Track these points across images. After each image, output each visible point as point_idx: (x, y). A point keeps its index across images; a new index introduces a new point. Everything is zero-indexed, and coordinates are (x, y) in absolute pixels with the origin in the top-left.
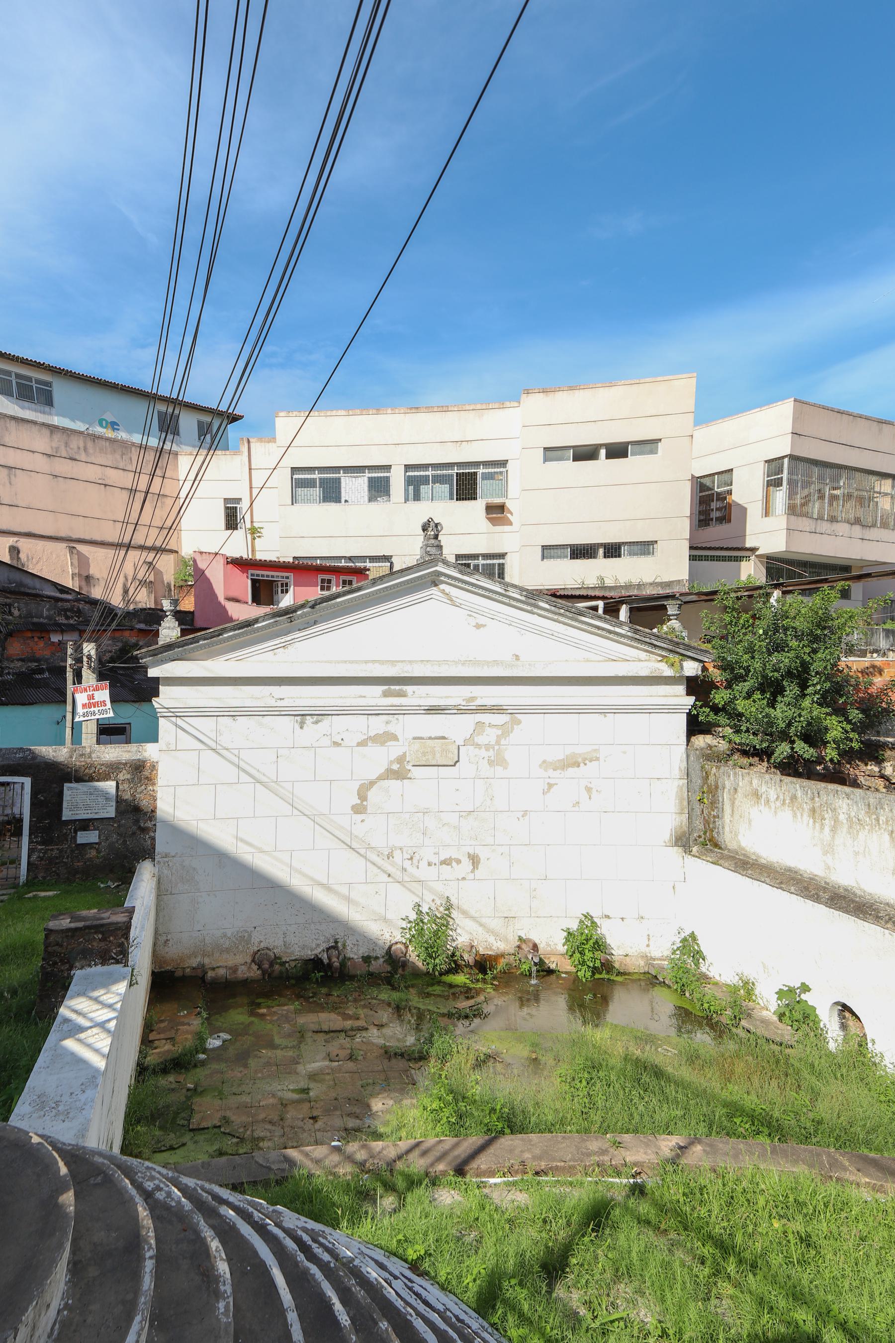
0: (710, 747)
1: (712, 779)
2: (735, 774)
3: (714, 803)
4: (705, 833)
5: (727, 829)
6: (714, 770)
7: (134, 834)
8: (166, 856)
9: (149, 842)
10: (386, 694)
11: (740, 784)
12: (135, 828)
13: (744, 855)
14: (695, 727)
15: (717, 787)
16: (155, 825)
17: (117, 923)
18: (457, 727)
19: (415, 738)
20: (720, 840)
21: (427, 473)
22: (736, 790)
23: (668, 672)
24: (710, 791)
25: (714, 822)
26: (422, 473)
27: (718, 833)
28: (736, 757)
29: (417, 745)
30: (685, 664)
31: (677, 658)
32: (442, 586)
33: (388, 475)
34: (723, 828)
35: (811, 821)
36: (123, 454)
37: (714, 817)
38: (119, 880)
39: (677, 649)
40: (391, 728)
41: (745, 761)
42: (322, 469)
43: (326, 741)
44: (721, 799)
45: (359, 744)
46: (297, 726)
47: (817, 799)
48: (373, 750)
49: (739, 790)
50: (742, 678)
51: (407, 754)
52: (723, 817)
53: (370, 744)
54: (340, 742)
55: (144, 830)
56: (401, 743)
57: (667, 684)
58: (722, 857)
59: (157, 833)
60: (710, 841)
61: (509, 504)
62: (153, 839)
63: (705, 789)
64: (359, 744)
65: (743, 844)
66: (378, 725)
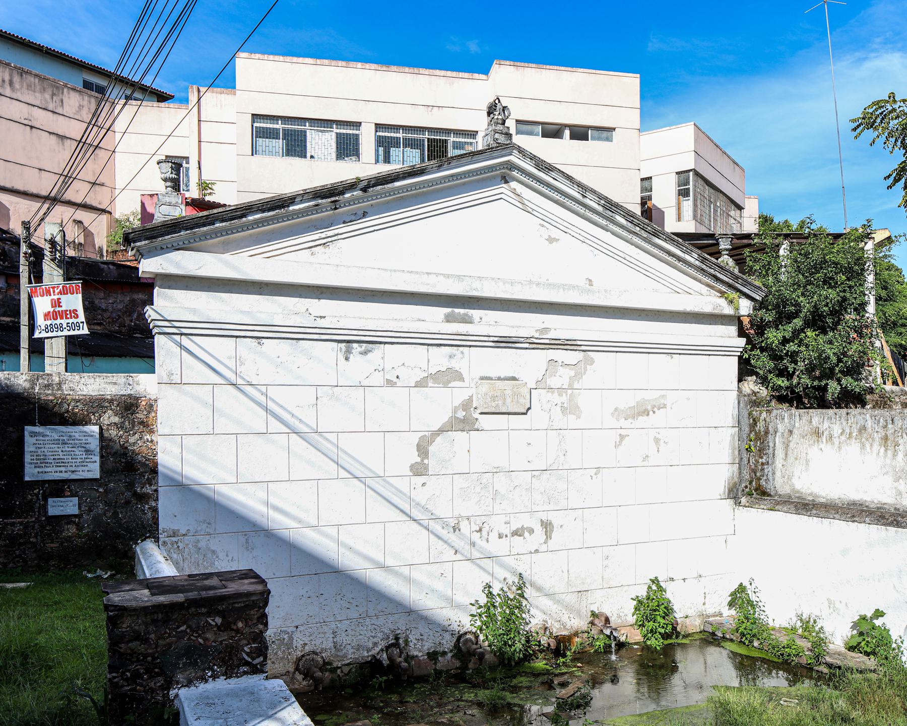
0: (754, 392)
1: (760, 426)
3: (761, 451)
4: (751, 483)
5: (778, 474)
6: (764, 415)
7: (128, 502)
8: (174, 534)
9: (150, 515)
11: (797, 425)
12: (128, 494)
14: (745, 369)
15: (767, 432)
16: (156, 491)
18: (528, 365)
19: (482, 378)
20: (769, 487)
22: (791, 432)
23: (728, 310)
24: (758, 437)
25: (763, 470)
27: (767, 480)
28: (773, 403)
29: (485, 387)
30: (740, 300)
31: (733, 295)
34: (774, 474)
38: (111, 568)
39: (732, 287)
40: (455, 364)
43: (378, 379)
44: (771, 445)
45: (420, 384)
48: (434, 392)
49: (795, 431)
51: (474, 399)
52: (773, 463)
53: (430, 384)
54: (395, 380)
55: (143, 498)
56: (466, 384)
59: (160, 502)
60: (756, 490)
62: (155, 510)
63: (752, 436)
64: (420, 384)
66: (439, 358)
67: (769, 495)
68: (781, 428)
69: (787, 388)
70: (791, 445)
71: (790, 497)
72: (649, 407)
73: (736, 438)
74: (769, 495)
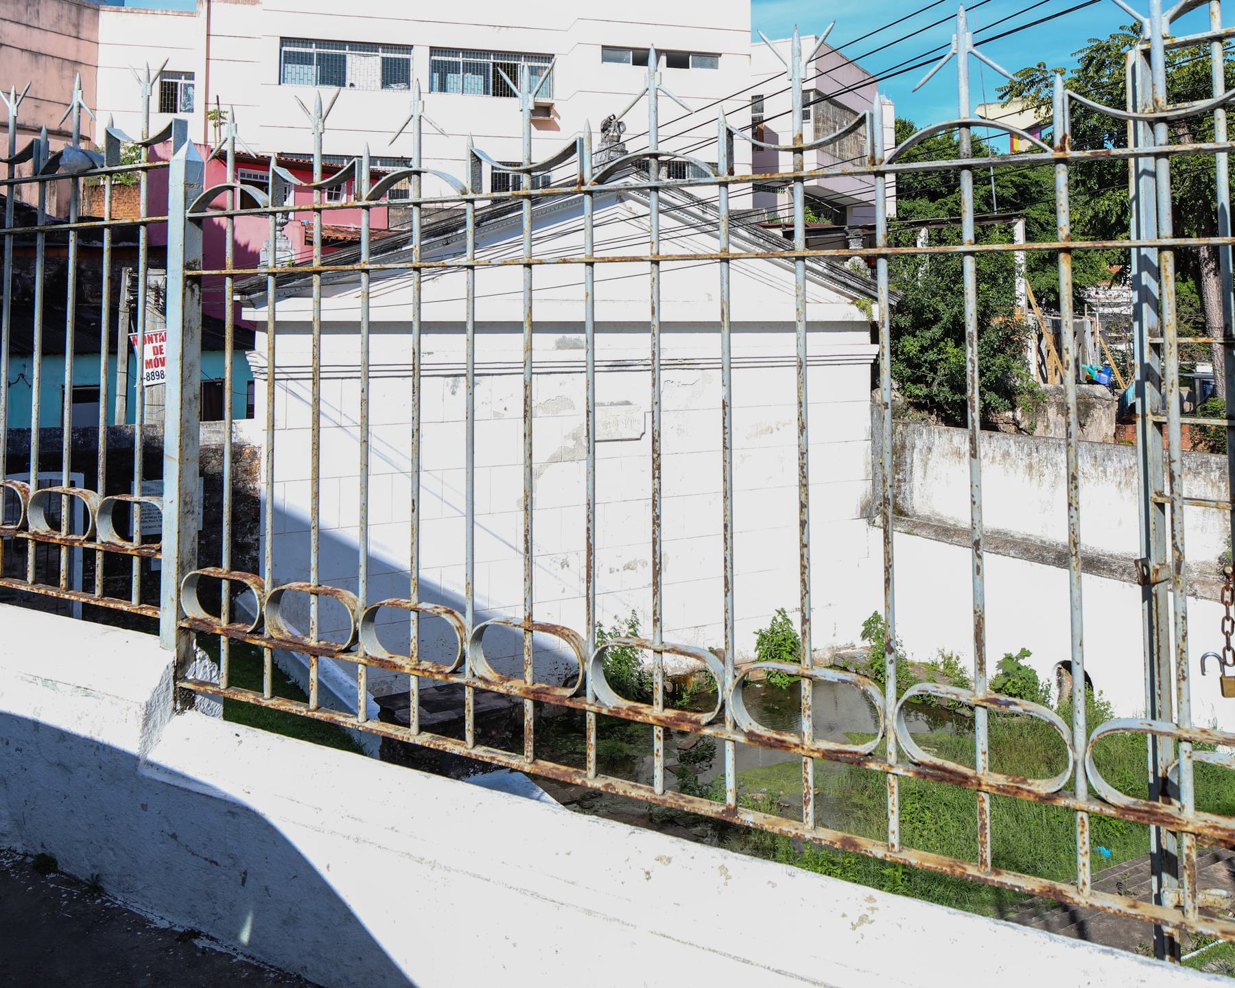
2: (930, 431)
10: (561, 346)
13: (939, 521)
15: (903, 447)
17: (501, 710)
20: (906, 506)
21: (457, 59)
22: (930, 449)
25: (899, 487)
26: (450, 59)
28: (910, 412)
32: (629, 203)
33: (407, 56)
34: (911, 492)
35: (1027, 477)
36: (28, 5)
37: (899, 480)
41: (919, 415)
42: (321, 43)
44: (908, 460)
46: (448, 391)
47: (1035, 454)
50: (928, 325)
52: (911, 480)
57: (853, 330)
58: (916, 526)
61: (556, 108)
65: (937, 510)
67: (907, 515)
68: (919, 443)
69: (926, 396)
70: (930, 463)
71: (929, 519)
72: (774, 426)
73: (870, 452)
74: (907, 515)
